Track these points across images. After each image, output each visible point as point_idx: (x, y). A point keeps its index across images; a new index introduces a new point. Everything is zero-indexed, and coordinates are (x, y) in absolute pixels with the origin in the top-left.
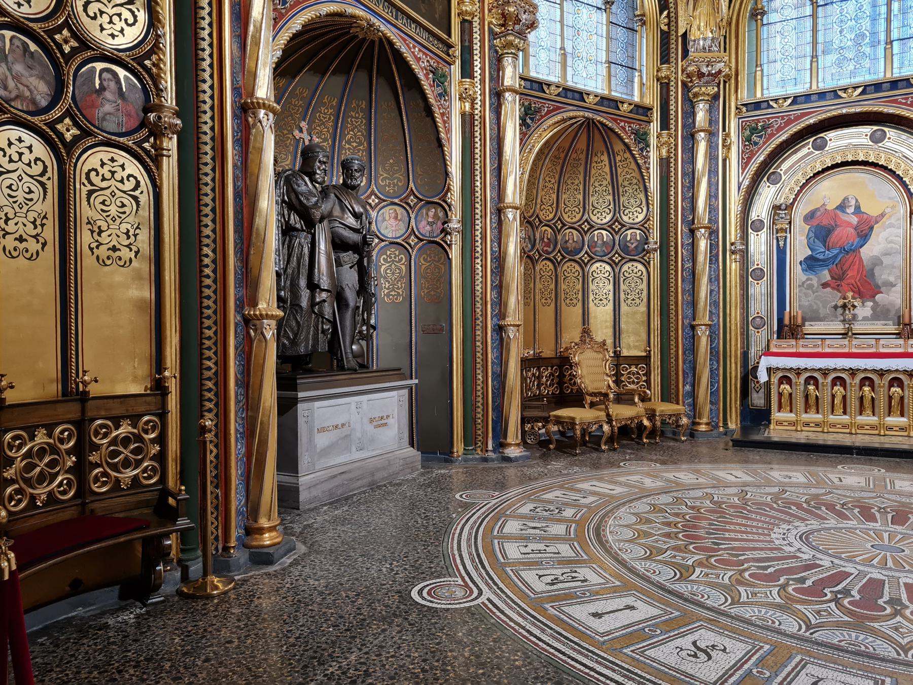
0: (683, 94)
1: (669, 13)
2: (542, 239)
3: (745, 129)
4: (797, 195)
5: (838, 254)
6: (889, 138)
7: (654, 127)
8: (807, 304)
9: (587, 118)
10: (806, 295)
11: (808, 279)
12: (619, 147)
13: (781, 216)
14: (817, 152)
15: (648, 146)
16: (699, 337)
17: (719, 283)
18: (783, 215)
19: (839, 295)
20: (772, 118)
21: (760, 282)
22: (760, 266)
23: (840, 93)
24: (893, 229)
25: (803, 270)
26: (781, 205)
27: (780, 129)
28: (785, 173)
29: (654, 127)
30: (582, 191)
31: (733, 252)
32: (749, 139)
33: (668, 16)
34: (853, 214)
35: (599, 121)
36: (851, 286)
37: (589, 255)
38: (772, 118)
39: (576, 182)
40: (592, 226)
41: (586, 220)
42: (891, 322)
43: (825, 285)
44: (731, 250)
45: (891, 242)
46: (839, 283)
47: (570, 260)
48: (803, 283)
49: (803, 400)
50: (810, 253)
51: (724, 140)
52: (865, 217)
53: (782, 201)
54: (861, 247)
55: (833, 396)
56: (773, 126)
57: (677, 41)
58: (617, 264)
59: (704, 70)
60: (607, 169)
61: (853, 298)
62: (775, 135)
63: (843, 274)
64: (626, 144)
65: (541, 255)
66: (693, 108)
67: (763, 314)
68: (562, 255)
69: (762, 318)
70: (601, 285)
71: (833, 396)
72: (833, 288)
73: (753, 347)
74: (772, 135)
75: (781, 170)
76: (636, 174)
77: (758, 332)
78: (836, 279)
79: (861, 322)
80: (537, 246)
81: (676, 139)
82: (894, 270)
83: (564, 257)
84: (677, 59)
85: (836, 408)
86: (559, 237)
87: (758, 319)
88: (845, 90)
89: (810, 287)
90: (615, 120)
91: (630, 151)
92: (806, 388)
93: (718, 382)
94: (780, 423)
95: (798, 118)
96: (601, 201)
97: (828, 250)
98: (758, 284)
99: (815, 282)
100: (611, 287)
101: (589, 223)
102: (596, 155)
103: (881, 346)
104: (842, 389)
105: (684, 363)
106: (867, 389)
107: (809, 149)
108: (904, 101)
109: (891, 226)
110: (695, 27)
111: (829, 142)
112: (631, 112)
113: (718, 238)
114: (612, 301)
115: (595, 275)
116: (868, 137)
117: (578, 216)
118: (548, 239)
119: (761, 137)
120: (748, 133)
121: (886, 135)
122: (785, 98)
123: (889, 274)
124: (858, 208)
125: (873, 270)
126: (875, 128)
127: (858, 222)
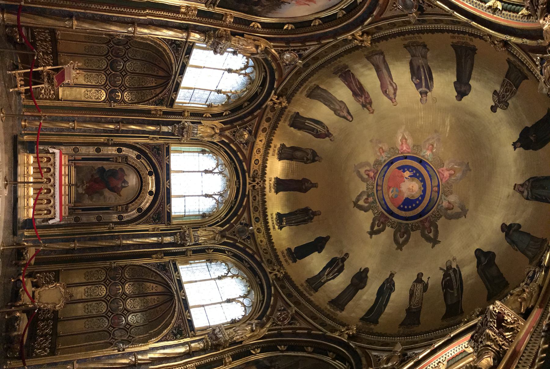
0: (176, 121)
1: (210, 117)
2: (119, 49)
7: (164, 108)
9: (171, 76)
12: (158, 91)
15: (157, 105)
27: (157, 159)
29: (164, 108)
30: (141, 72)
32: (155, 147)
33: (209, 117)
35: (169, 82)
37: (110, 74)
39: (145, 70)
40: (124, 76)
41: (126, 74)
47: (108, 63)
51: (155, 138)
57: (199, 120)
58: (105, 87)
59: (185, 130)
60: (149, 85)
64: (157, 95)
65: (111, 48)
66: (170, 125)
68: (110, 59)
70: (95, 79)
74: (155, 156)
76: (146, 99)
80: (115, 46)
81: (158, 118)
83: (109, 61)
84: (191, 119)
86: (119, 59)
90: (169, 90)
91: (155, 97)
95: (161, 166)
96: (135, 82)
100: (94, 84)
101: (125, 75)
102: (155, 80)
105: (56, 116)
110: (202, 127)
112: (172, 98)
114: (86, 83)
115: (100, 76)
117: (128, 70)
118: (119, 53)
120: (158, 147)
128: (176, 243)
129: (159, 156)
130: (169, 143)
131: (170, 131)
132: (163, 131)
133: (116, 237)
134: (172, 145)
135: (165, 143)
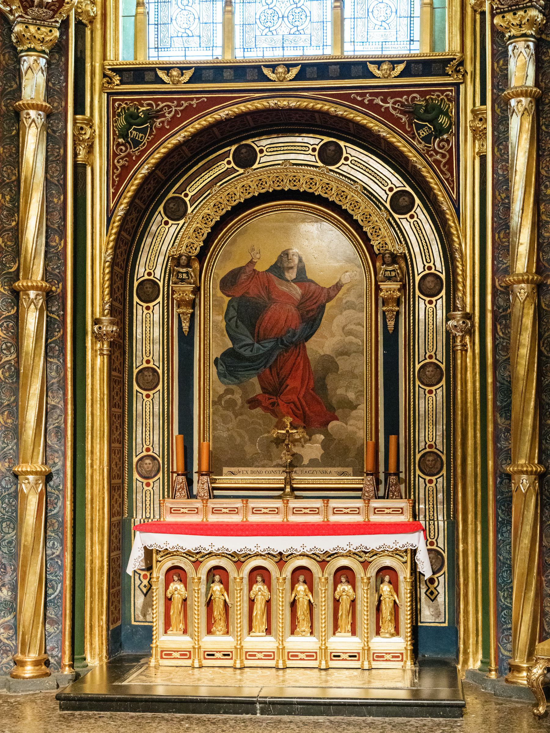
3: (119, 115)
4: (208, 241)
5: (273, 349)
6: (346, 159)
8: (225, 435)
10: (225, 419)
11: (227, 391)
13: (180, 276)
14: (241, 171)
16: (25, 497)
17: (65, 394)
18: (185, 276)
19: (275, 420)
20: (163, 100)
21: (151, 393)
22: (151, 365)
23: (266, 71)
24: (352, 311)
25: (219, 374)
26: (181, 256)
27: (174, 122)
28: (192, 201)
31: (97, 337)
34: (295, 281)
36: (292, 406)
38: (163, 100)
42: (350, 470)
43: (253, 403)
44: (93, 332)
45: (350, 333)
46: (274, 399)
48: (221, 397)
49: (203, 610)
50: (230, 345)
51: (79, 130)
52: (313, 287)
53: (183, 250)
54: (307, 338)
55: (252, 602)
56: (163, 116)
61: (293, 427)
62: (169, 130)
63: (281, 384)
66: (18, 61)
67: (156, 451)
69: (154, 458)
71: (252, 602)
72: (266, 409)
73: (140, 512)
74: (162, 131)
75: (186, 195)
77: (148, 485)
78: (270, 393)
79: (308, 469)
82: (355, 381)
85: (255, 623)
87: (148, 461)
88: (273, 67)
89: (231, 404)
92: (208, 589)
93: (63, 582)
94: (167, 654)
95: (203, 106)
97: (258, 342)
98: (148, 396)
99: (238, 397)
103: (330, 511)
104: (264, 588)
106: (301, 588)
107: (229, 163)
108: (359, 98)
109: (351, 306)
111: (259, 155)
113: (64, 309)
116: (316, 153)
119: (144, 131)
120: (122, 122)
121: (342, 153)
122: (182, 69)
123: (347, 388)
124: (302, 270)
125: (324, 379)
126: (326, 139)
127: (303, 296)
128: (540, 31)
129: (159, 114)
130: (103, 67)
131: (43, 62)
132: (42, 96)
133: (501, 302)
134: (110, 55)
135: (103, 88)
